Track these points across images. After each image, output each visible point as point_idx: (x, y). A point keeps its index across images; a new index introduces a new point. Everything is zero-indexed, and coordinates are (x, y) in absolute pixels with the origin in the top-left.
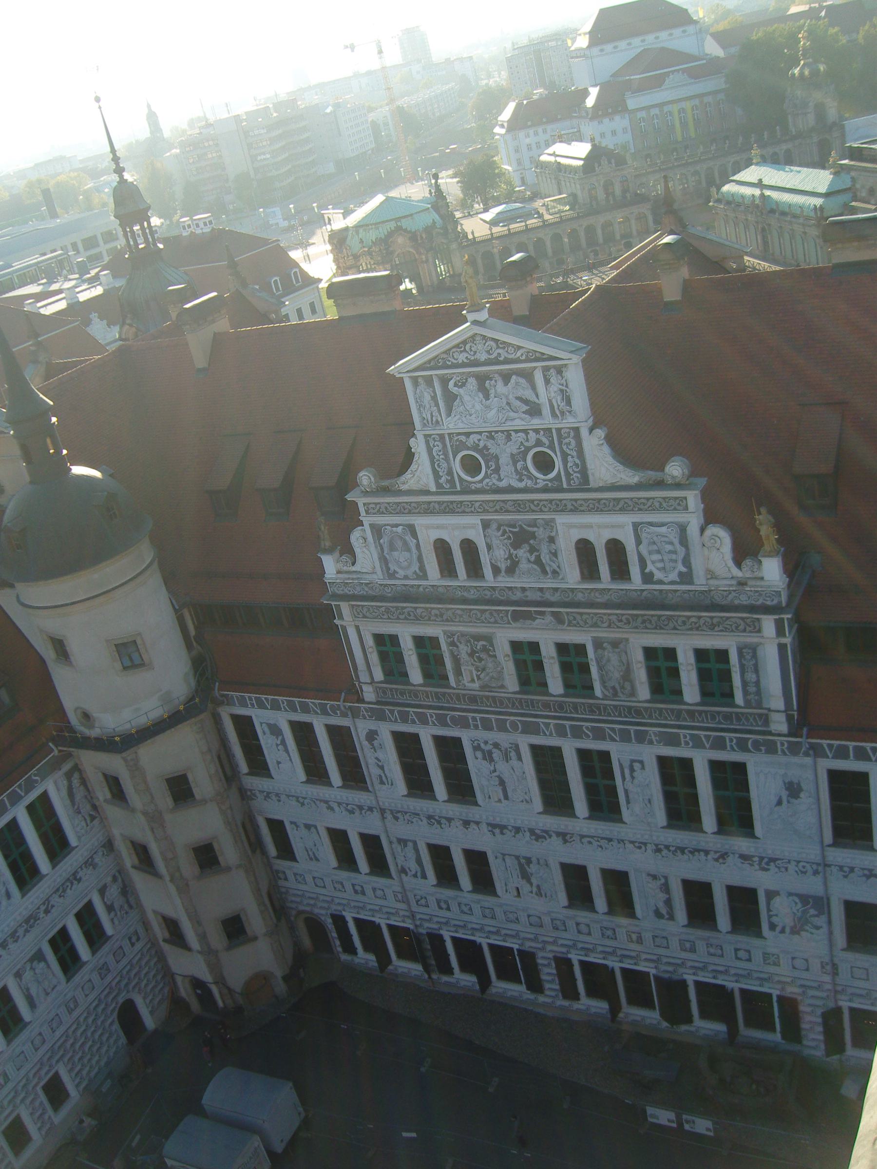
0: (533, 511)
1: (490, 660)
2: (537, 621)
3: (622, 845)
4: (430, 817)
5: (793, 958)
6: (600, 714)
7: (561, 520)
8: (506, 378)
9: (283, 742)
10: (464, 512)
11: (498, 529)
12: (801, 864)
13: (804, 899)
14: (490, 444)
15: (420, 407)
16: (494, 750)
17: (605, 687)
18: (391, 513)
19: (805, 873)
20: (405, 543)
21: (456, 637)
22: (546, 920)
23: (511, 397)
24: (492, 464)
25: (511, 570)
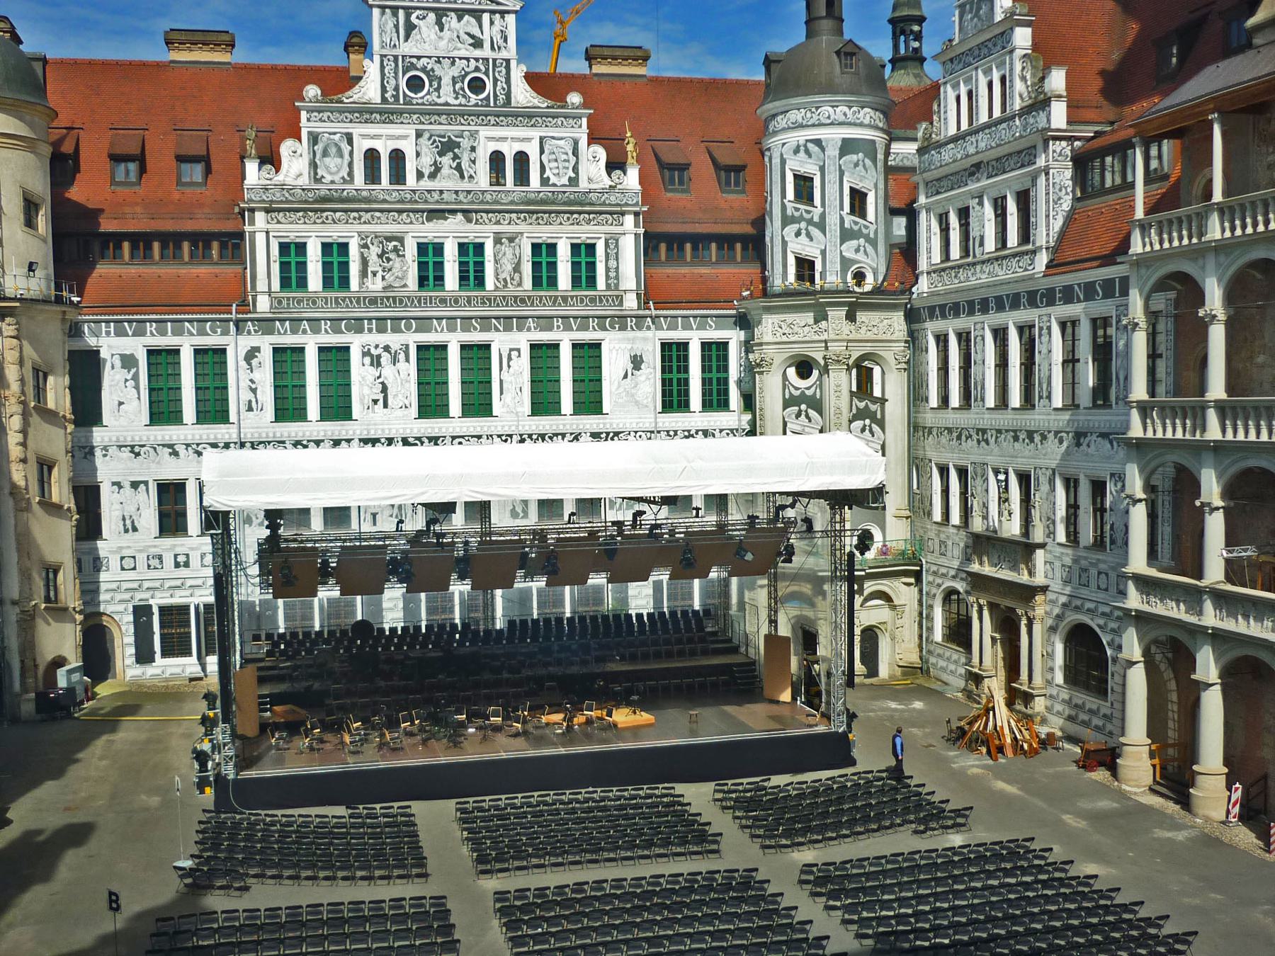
1: (398, 260)
7: (484, 132)
8: (460, 19)
9: (136, 378)
14: (436, 67)
15: (382, 31)
24: (435, 84)
25: (433, 176)
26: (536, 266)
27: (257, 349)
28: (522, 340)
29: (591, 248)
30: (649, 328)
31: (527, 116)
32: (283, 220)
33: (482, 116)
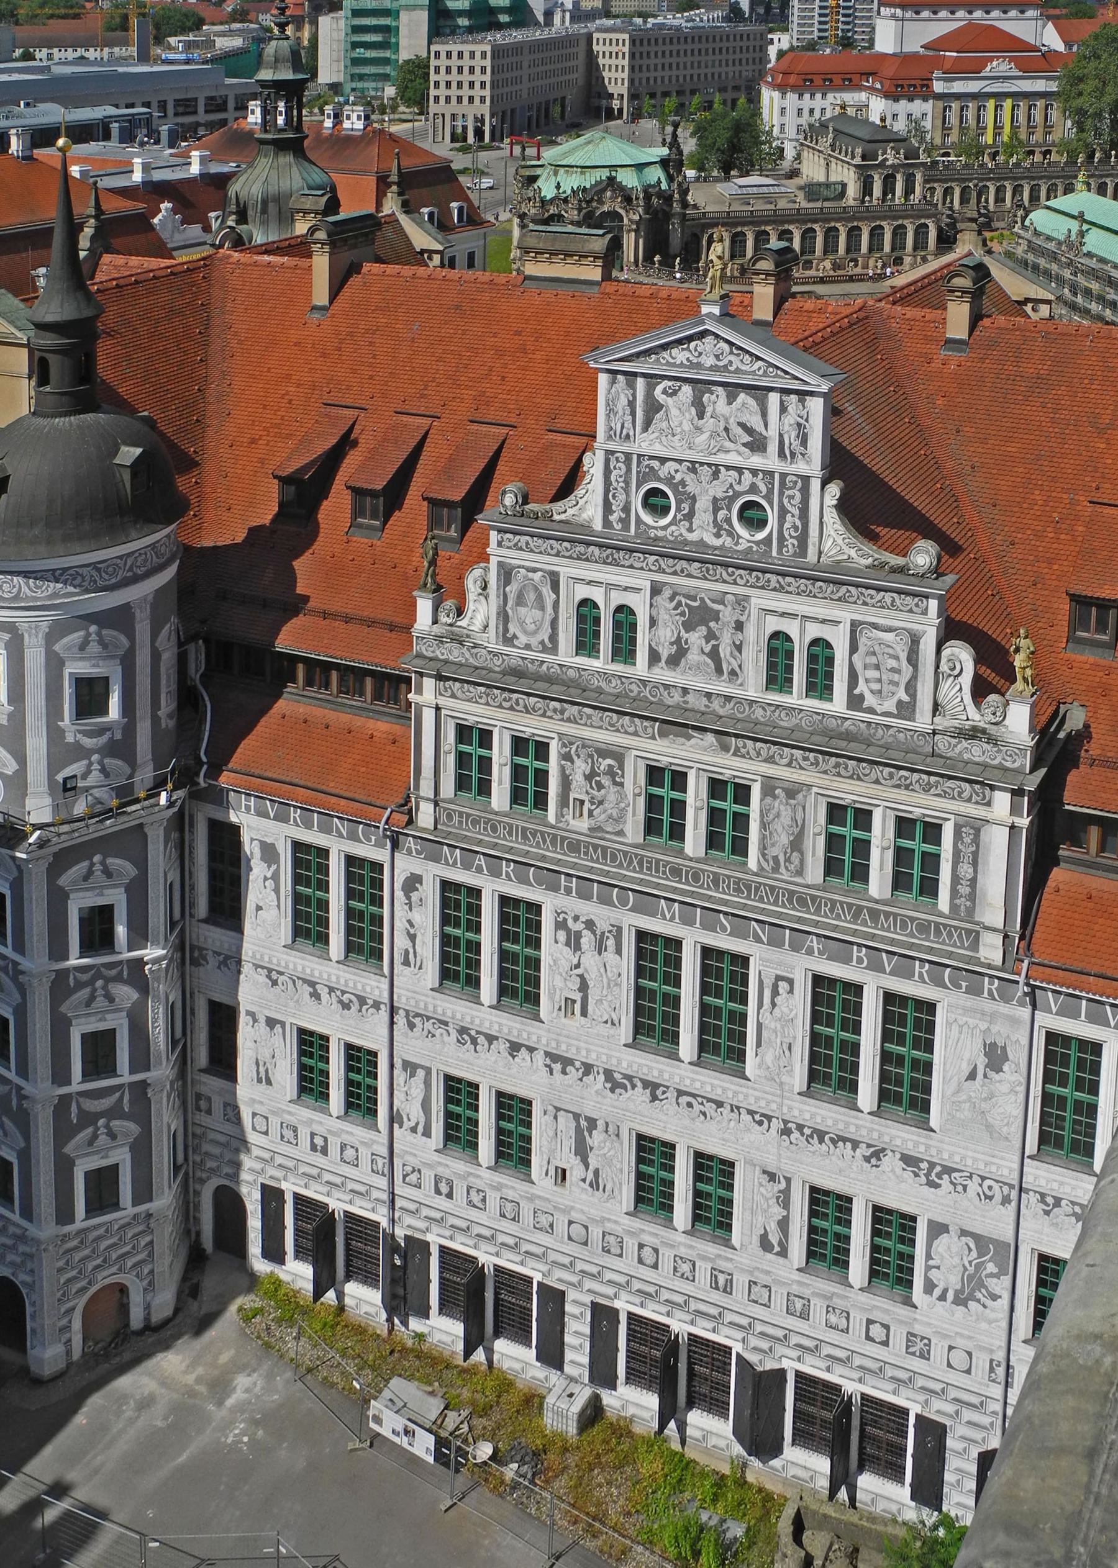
0: (725, 582)
2: (693, 741)
3: (735, 1115)
4: (463, 1031)
5: (951, 1348)
6: (748, 897)
7: (759, 600)
10: (631, 567)
11: (672, 599)
12: (987, 1183)
13: (981, 1242)
16: (585, 932)
17: (764, 855)
18: (532, 551)
19: (991, 1198)
20: (540, 597)
21: (574, 748)
22: (596, 1232)
23: (732, 420)
24: (686, 507)
25: (674, 661)
28: (801, 966)
31: (833, 579)
32: (459, 694)
33: (755, 568)
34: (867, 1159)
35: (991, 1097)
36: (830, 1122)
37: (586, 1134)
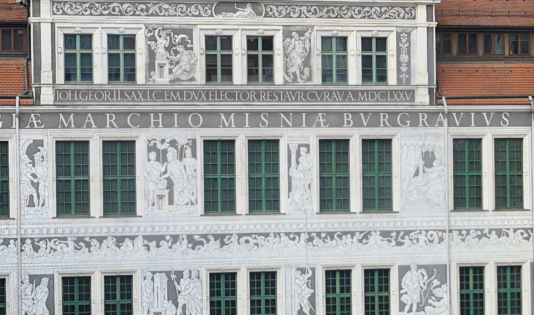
1: (186, 53)
2: (238, 13)
3: (277, 239)
4: (79, 240)
6: (279, 101)
12: (430, 233)
13: (430, 269)
17: (287, 73)
19: (431, 241)
21: (157, 31)
26: (326, 60)
27: (40, 143)
29: (382, 42)
30: (441, 124)
32: (69, 11)
34: (360, 241)
35: (428, 182)
36: (336, 225)
37: (176, 283)
